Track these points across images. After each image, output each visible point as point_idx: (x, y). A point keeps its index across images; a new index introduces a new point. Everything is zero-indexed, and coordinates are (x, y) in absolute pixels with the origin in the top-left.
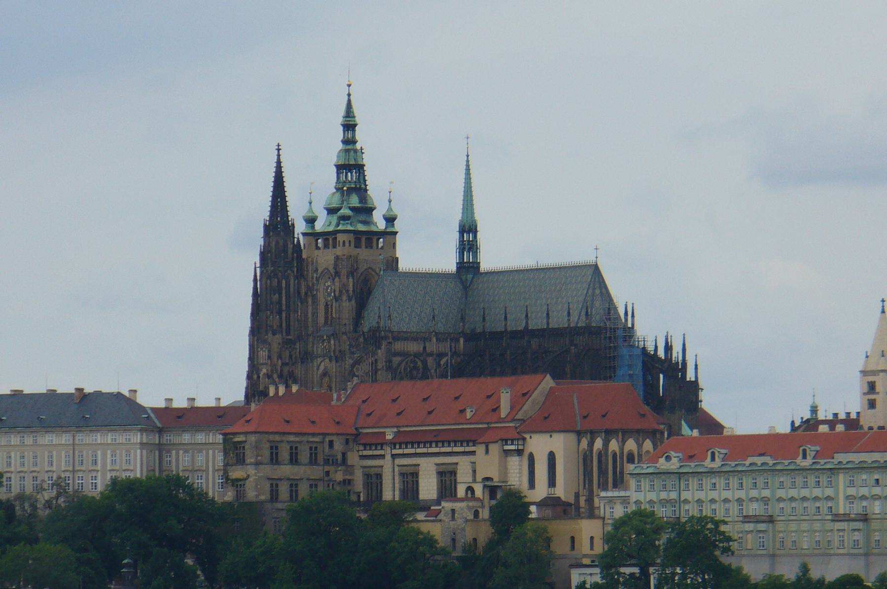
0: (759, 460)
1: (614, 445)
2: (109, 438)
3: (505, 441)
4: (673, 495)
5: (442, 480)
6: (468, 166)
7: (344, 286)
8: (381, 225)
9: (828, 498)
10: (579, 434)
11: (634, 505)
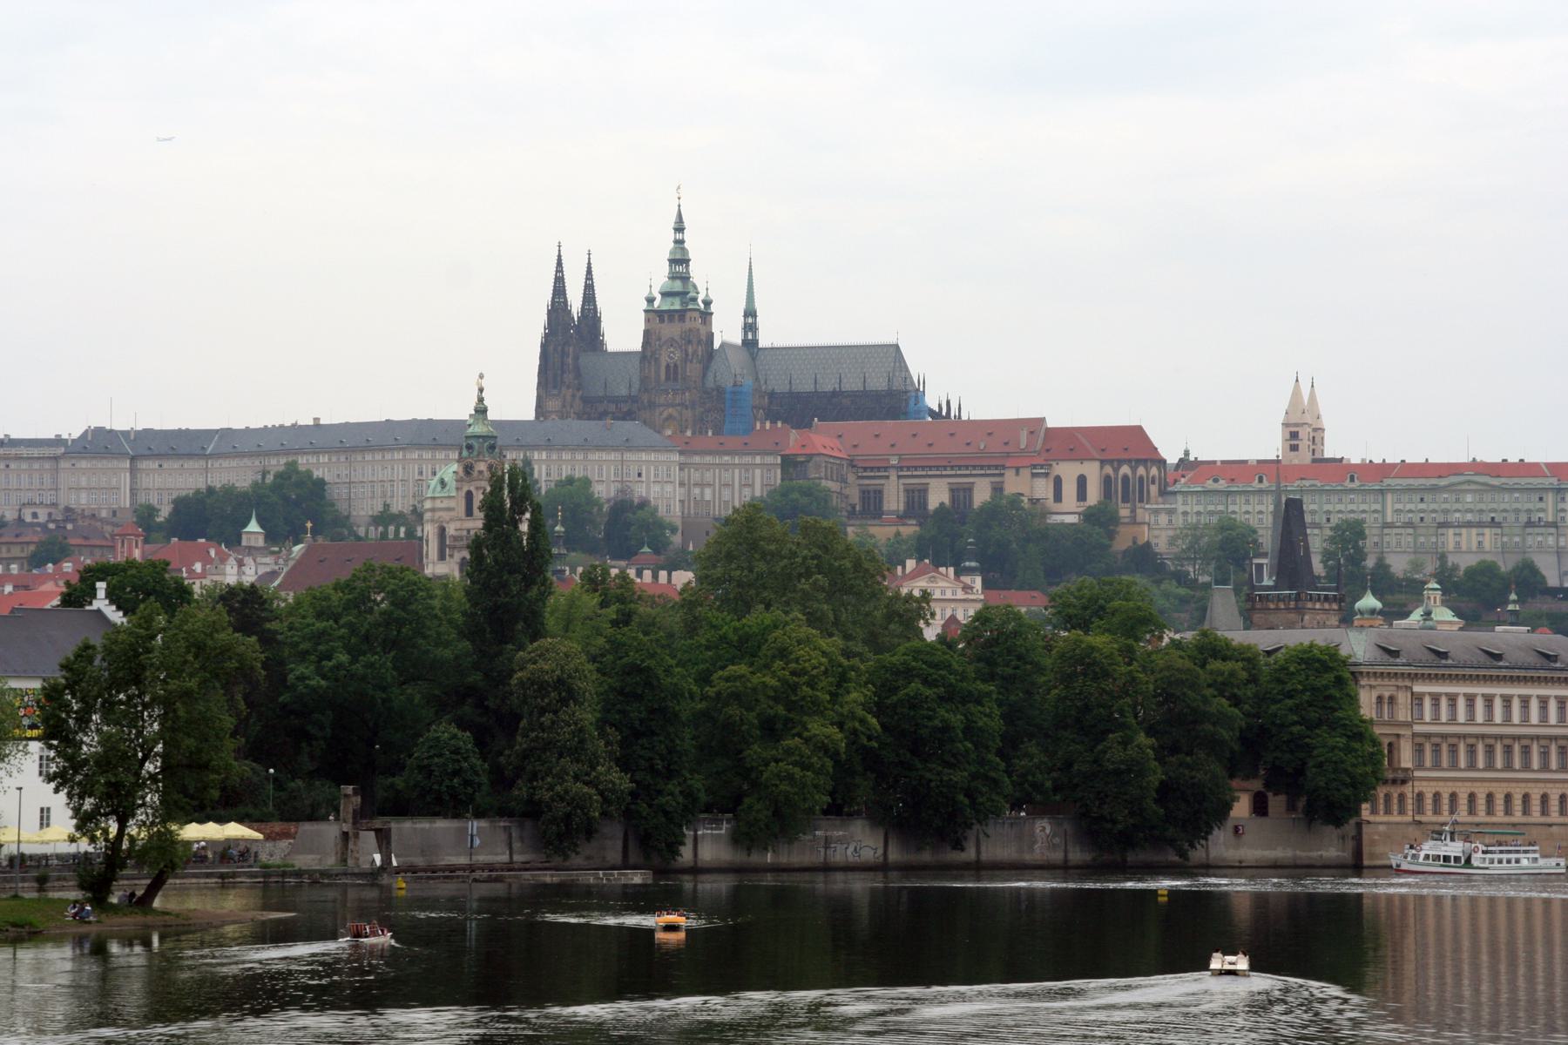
0: (1307, 483)
1: (1141, 471)
2: (653, 457)
3: (1034, 467)
4: (1221, 508)
5: (953, 496)
6: (750, 266)
7: (695, 352)
8: (702, 306)
9: (1375, 511)
10: (1103, 462)
11: (1181, 517)
